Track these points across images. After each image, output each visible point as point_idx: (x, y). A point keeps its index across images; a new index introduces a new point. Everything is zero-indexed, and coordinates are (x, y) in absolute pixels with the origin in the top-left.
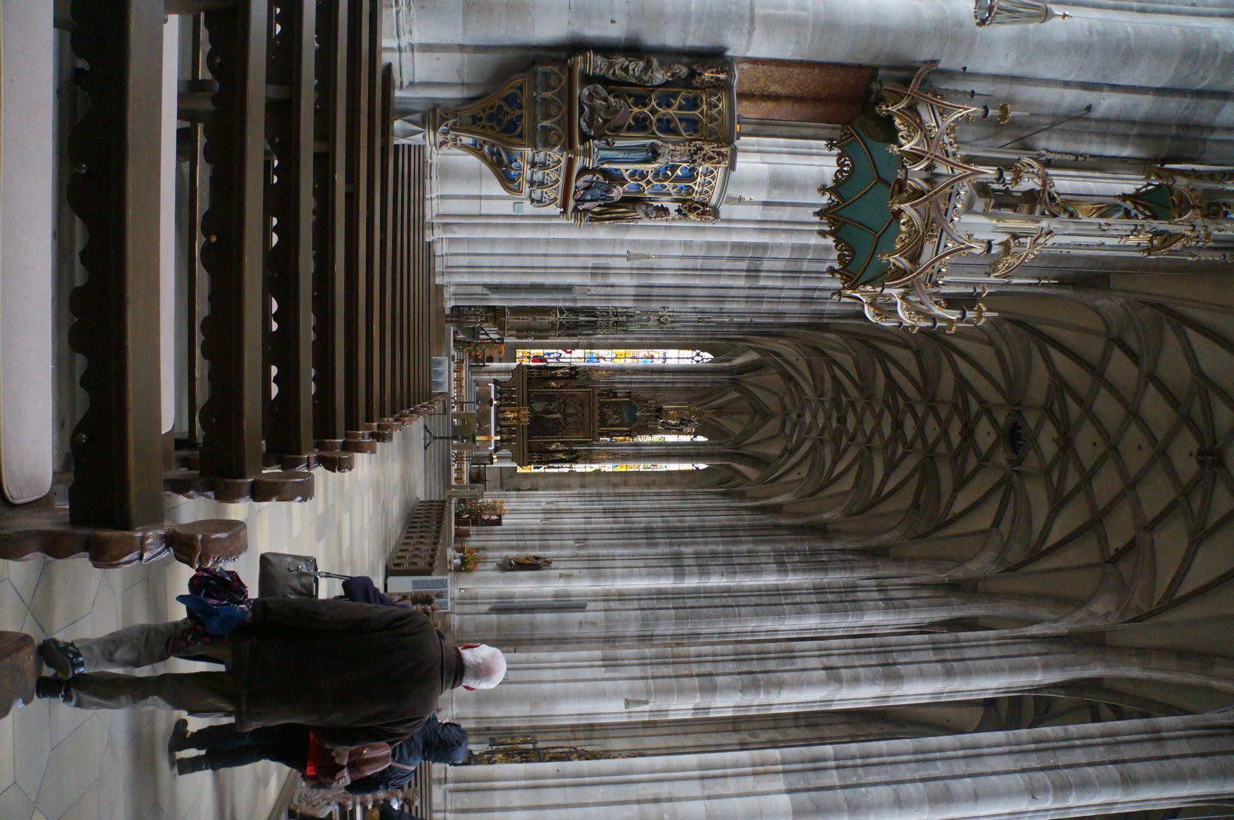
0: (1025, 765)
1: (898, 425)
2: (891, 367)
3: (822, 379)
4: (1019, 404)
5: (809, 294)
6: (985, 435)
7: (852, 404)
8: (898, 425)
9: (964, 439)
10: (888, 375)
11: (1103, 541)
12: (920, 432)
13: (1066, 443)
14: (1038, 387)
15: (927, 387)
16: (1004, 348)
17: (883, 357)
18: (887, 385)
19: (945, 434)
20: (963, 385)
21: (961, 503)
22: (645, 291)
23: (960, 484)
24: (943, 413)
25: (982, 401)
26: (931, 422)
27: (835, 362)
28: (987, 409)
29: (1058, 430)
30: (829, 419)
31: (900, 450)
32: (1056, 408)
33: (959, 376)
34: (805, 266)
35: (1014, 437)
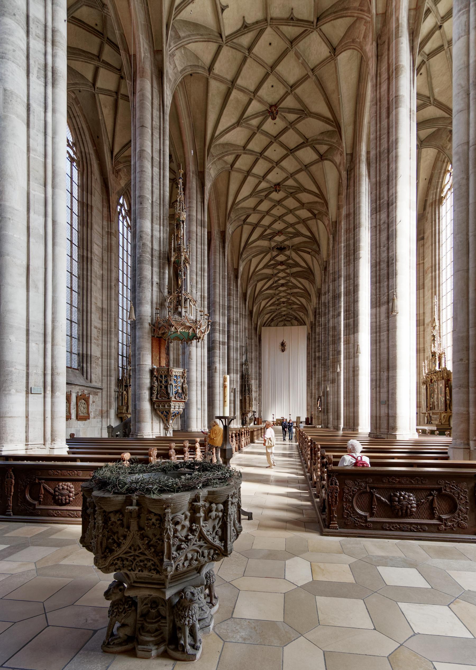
0: (352, 260)
1: (282, 285)
2: (263, 289)
3: (271, 309)
4: (270, 248)
5: (235, 322)
6: (281, 258)
7: (278, 300)
8: (282, 285)
9: (284, 265)
10: (267, 289)
11: (309, 219)
12: (283, 278)
13: (280, 232)
14: (264, 243)
15: (269, 277)
16: (252, 255)
17: (260, 292)
18: (270, 290)
19: (283, 270)
20: (266, 266)
21: (303, 264)
22: (235, 371)
23: (297, 265)
24: (276, 272)
25: (270, 260)
26: (280, 275)
27: (264, 307)
28: (273, 258)
29: (276, 236)
30: (284, 307)
31: (290, 284)
32: (270, 237)
33: (263, 268)
34: (221, 328)
35: (281, 249)
